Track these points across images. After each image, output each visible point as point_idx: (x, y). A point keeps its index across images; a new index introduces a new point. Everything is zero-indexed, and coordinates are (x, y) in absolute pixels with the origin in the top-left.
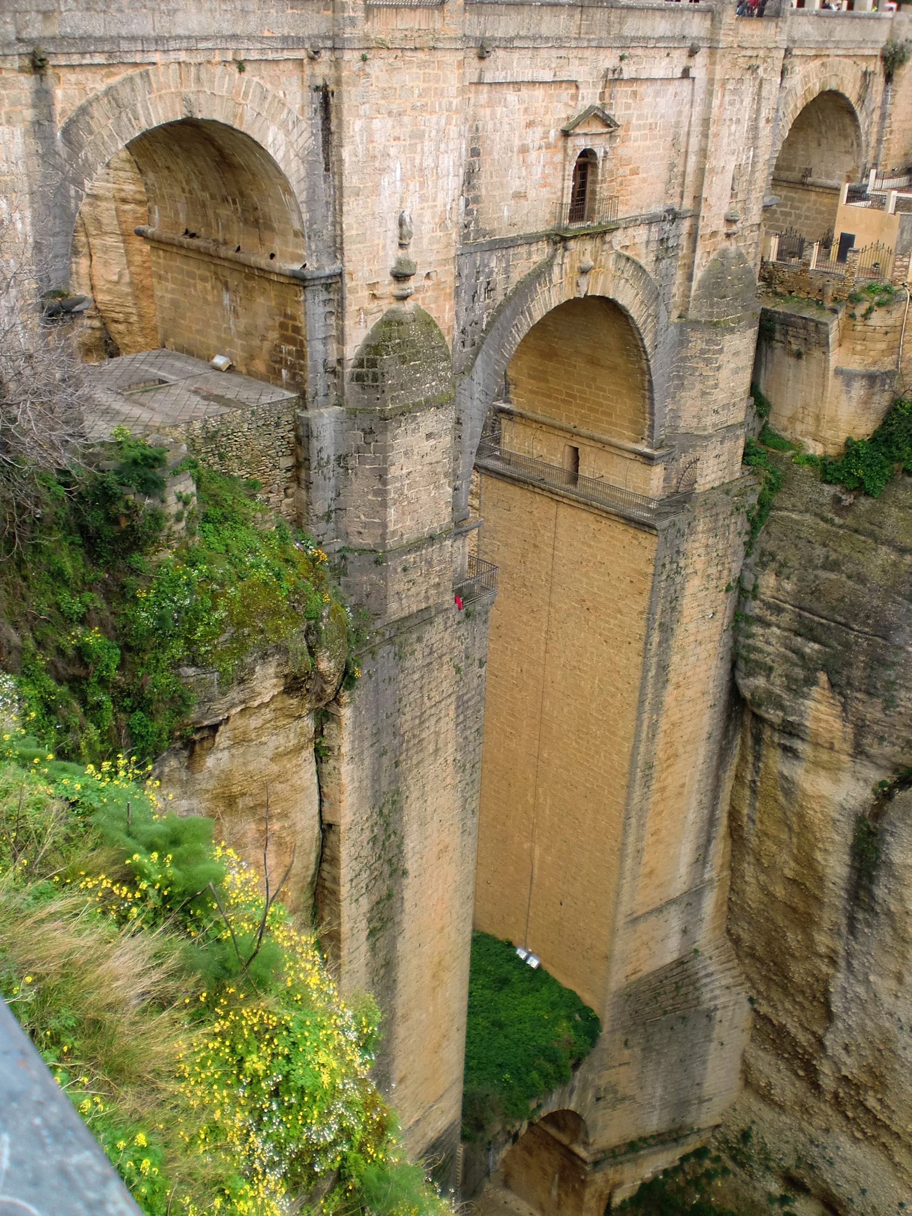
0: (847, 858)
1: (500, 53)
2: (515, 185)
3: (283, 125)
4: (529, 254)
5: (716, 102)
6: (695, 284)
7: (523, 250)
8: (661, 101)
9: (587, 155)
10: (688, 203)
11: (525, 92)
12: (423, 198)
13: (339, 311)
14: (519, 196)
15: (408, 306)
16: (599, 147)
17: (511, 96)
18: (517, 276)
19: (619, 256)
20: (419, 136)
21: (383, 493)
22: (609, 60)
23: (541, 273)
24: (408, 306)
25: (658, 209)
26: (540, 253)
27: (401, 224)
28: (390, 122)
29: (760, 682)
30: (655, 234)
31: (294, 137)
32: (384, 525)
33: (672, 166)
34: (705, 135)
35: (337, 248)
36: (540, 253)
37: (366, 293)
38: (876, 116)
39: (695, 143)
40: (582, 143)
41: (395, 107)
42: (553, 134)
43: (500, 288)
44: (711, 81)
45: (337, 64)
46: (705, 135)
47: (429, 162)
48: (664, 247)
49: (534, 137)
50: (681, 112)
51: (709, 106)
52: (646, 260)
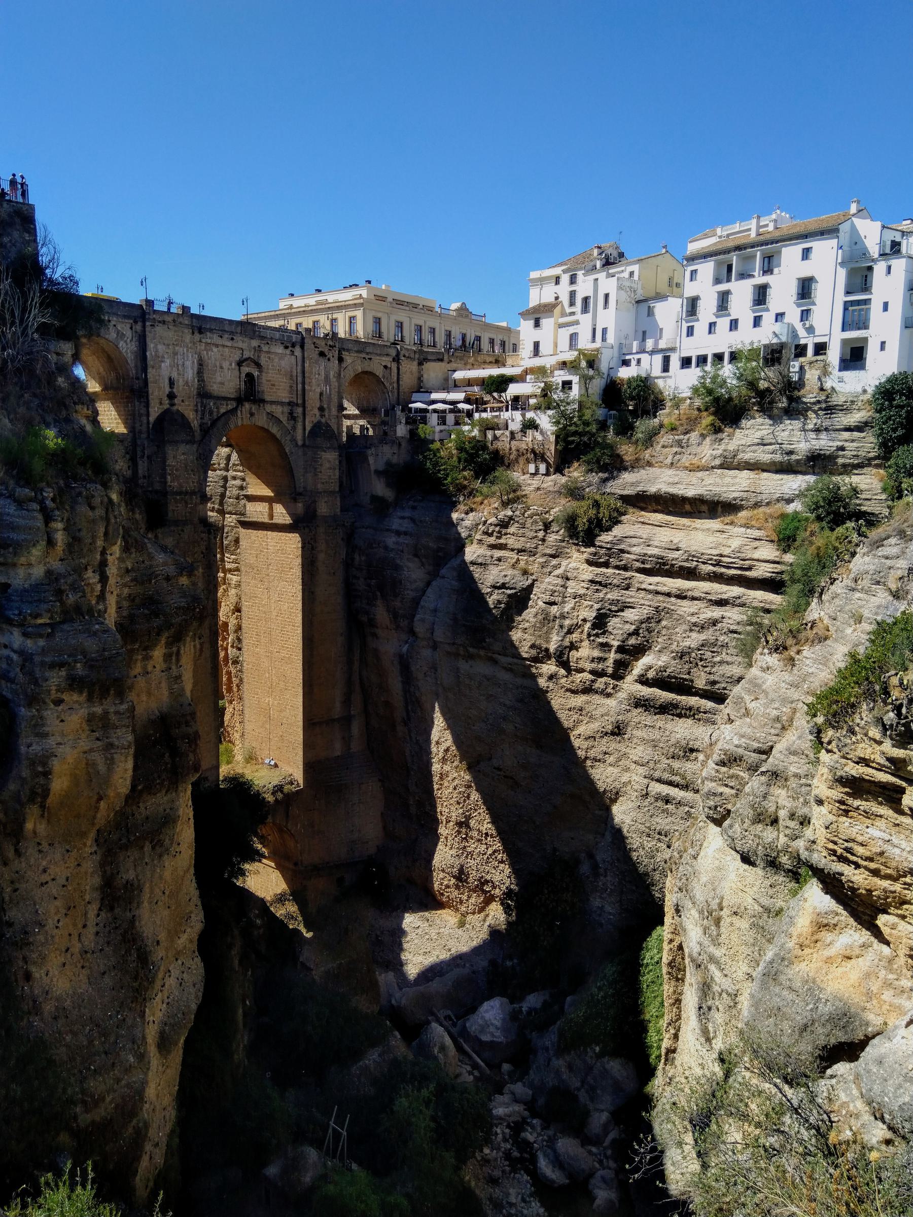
0: (400, 679)
1: (208, 334)
2: (219, 379)
3: (126, 342)
4: (227, 405)
5: (307, 365)
6: (307, 432)
7: (225, 403)
8: (283, 363)
10: (300, 402)
11: (220, 348)
12: (179, 374)
13: (147, 406)
14: (222, 384)
15: (175, 408)
18: (222, 411)
20: (175, 354)
21: (164, 469)
22: (255, 343)
23: (233, 411)
24: (175, 408)
25: (287, 400)
26: (231, 405)
27: (170, 379)
28: (164, 347)
30: (286, 409)
31: (129, 346)
32: (166, 482)
33: (291, 387)
34: (304, 377)
37: (158, 401)
38: (395, 385)
39: (300, 379)
41: (166, 342)
43: (215, 414)
44: (303, 358)
45: (144, 327)
46: (304, 377)
47: (180, 362)
48: (292, 417)
50: (292, 368)
51: (303, 367)
52: (284, 419)
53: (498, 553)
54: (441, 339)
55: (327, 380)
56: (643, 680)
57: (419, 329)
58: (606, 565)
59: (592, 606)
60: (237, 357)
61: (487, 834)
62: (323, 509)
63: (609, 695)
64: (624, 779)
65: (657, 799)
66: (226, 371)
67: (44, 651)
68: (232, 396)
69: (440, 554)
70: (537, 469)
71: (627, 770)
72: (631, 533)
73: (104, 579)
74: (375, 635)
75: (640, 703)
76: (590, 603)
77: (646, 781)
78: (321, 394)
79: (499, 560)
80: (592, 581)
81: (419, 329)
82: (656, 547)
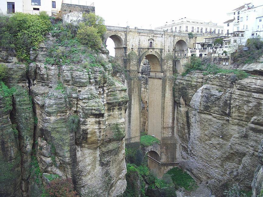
9: (151, 42)
16: (152, 42)
17: (143, 36)
19: (155, 51)
26: (147, 50)
29: (176, 98)
35: (126, 46)
36: (147, 50)
39: (164, 43)
40: (151, 41)
42: (148, 40)
49: (145, 40)
53: (213, 86)
54: (204, 31)
55: (171, 42)
56: (253, 123)
57: (198, 28)
58: (243, 90)
59: (239, 102)
60: (148, 38)
61: (208, 161)
62: (168, 74)
63: (243, 127)
64: (247, 150)
65: (256, 157)
66: (145, 41)
67: (86, 106)
68: (146, 48)
69: (197, 86)
70: (226, 64)
71: (248, 148)
72: (251, 82)
73: (103, 90)
74: (180, 107)
75: (252, 129)
76: (238, 101)
77: (253, 151)
78: (169, 46)
79: (213, 88)
80: (238, 94)
81: (198, 28)
82: (259, 85)
